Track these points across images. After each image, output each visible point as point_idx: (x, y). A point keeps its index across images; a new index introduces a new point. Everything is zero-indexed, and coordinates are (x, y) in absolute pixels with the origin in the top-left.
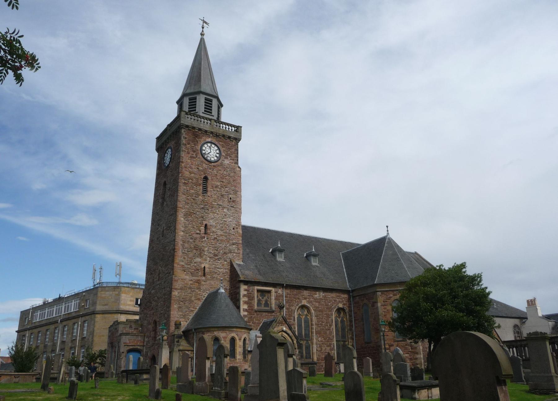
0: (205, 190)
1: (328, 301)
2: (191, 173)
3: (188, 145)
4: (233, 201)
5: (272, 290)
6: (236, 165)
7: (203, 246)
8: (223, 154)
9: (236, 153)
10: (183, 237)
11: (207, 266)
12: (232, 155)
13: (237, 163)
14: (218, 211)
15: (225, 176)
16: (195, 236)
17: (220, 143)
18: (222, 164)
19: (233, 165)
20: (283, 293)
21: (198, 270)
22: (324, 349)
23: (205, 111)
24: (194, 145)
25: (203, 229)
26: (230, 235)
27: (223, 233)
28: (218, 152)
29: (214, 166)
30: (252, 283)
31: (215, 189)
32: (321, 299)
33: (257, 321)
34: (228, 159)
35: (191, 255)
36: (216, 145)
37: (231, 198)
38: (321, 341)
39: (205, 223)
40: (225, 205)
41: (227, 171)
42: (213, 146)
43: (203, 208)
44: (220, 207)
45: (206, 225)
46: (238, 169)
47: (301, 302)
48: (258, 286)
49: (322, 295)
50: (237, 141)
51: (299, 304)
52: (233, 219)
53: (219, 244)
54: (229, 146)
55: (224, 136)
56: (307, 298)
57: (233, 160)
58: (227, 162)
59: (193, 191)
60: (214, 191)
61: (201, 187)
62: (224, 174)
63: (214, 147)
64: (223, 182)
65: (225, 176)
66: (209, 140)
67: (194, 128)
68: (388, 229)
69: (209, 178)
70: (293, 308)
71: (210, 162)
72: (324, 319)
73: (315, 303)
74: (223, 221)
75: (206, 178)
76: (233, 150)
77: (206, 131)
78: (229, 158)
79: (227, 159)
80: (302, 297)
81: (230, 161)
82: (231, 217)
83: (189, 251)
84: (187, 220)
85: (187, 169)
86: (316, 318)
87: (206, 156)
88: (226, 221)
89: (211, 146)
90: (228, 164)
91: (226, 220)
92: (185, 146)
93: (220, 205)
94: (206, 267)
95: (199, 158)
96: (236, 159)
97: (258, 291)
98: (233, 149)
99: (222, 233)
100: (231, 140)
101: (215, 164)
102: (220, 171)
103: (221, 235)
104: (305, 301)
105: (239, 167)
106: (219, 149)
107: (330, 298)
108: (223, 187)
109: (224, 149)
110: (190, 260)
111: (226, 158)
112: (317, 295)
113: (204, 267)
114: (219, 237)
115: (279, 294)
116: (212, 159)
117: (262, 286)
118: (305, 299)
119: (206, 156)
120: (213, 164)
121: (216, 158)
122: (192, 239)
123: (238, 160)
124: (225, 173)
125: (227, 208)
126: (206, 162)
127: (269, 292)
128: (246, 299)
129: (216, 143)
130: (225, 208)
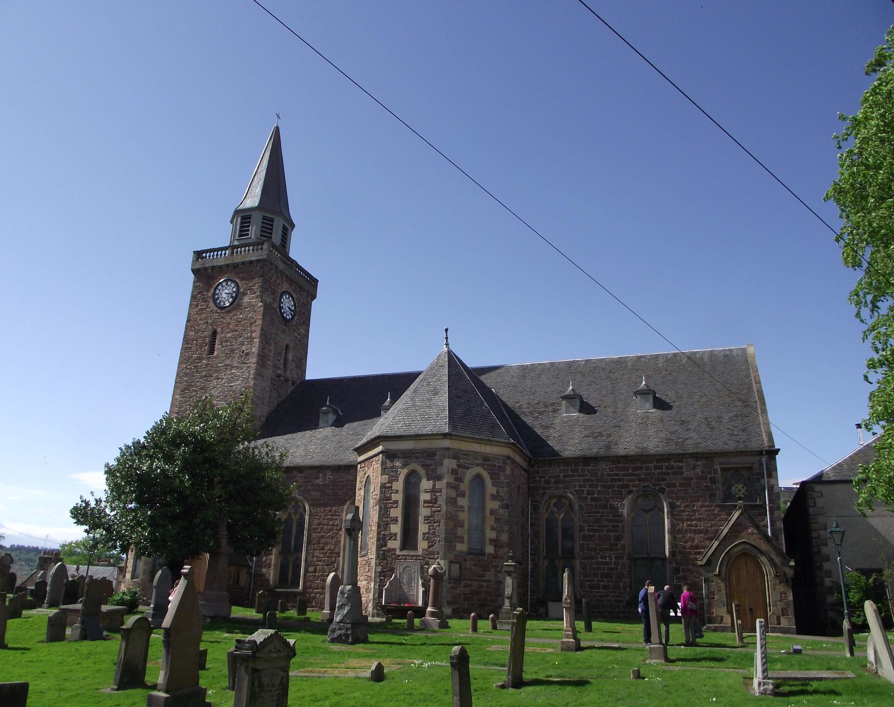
0: (212, 351)
4: (248, 354)
15: (241, 322)
17: (241, 275)
31: (224, 344)
32: (325, 485)
36: (233, 281)
40: (235, 364)
44: (227, 369)
55: (243, 263)
59: (196, 356)
60: (223, 347)
64: (236, 331)
65: (241, 322)
67: (206, 269)
68: (447, 335)
69: (219, 330)
73: (313, 493)
75: (215, 333)
85: (193, 329)
87: (218, 302)
93: (228, 366)
107: (343, 482)
109: (243, 282)
112: (319, 479)
119: (218, 302)
124: (241, 316)
125: (236, 367)
126: (219, 311)
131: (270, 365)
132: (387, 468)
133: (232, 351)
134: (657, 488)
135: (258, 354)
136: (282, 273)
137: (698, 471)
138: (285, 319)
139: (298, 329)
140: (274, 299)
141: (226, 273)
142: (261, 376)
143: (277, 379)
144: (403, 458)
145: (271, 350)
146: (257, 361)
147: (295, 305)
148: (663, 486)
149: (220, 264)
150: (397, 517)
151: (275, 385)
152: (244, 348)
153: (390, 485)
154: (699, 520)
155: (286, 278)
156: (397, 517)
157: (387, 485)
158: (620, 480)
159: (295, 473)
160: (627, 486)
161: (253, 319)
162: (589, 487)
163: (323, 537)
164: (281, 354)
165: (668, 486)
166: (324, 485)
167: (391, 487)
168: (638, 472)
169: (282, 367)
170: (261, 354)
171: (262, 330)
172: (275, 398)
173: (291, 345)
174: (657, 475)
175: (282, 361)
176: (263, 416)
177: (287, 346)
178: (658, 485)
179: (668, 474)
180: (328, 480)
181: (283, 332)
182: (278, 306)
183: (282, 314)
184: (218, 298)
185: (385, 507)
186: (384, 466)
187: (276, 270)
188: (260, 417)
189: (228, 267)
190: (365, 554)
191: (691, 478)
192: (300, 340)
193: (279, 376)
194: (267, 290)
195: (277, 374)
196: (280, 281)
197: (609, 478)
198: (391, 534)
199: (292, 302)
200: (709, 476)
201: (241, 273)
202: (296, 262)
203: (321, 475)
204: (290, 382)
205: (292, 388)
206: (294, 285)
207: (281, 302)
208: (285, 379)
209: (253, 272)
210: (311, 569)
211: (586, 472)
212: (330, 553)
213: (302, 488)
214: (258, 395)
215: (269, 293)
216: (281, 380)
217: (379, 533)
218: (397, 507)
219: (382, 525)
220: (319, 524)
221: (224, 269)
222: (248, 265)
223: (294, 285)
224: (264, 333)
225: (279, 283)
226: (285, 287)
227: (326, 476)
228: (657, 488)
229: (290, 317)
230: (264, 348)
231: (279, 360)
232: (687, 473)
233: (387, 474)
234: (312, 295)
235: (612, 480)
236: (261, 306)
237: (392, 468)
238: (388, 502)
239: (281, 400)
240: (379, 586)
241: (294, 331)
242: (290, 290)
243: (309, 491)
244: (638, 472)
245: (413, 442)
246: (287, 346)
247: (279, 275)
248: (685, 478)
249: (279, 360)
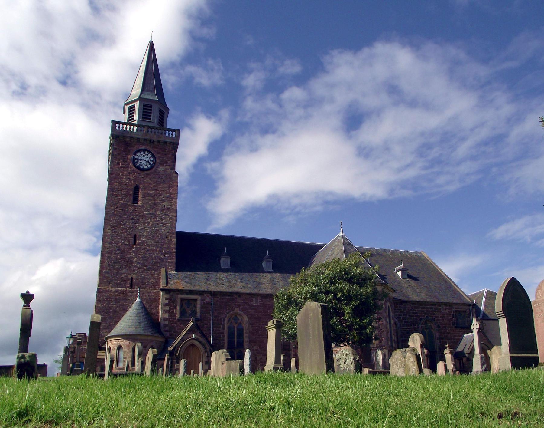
0: (136, 201)
1: (268, 308)
2: (121, 184)
3: (118, 156)
4: (168, 209)
5: (198, 298)
6: (173, 171)
7: (132, 257)
8: (158, 161)
9: (173, 158)
11: (134, 276)
12: (169, 161)
13: (174, 168)
14: (150, 220)
16: (122, 247)
17: (156, 149)
18: (156, 171)
19: (170, 171)
20: (211, 301)
21: (124, 281)
22: (258, 358)
23: (143, 118)
24: (126, 154)
25: (132, 240)
28: (152, 159)
29: (147, 174)
30: (175, 292)
33: (179, 330)
34: (163, 165)
35: (117, 266)
36: (150, 152)
37: (164, 206)
38: (256, 350)
41: (161, 178)
42: (147, 153)
43: (132, 219)
45: (135, 236)
46: (175, 175)
47: (233, 310)
48: (181, 294)
49: (260, 301)
50: (175, 145)
53: (149, 254)
54: (165, 151)
56: (241, 306)
57: (169, 166)
58: (161, 169)
61: (132, 198)
62: (159, 182)
63: (147, 155)
65: (160, 184)
66: (143, 147)
69: (141, 186)
70: (223, 316)
71: (143, 170)
72: (262, 327)
73: (250, 310)
75: (137, 189)
76: (170, 155)
77: (138, 139)
78: (164, 164)
79: (163, 166)
80: (235, 304)
81: (165, 167)
82: (165, 226)
84: (114, 232)
86: (251, 326)
88: (158, 230)
89: (145, 154)
90: (163, 171)
91: (158, 229)
92: (115, 157)
94: (133, 278)
95: (131, 167)
96: (173, 164)
97: (182, 300)
98: (169, 154)
99: (153, 242)
101: (148, 172)
102: (154, 179)
103: (152, 245)
104: (238, 308)
105: (176, 173)
106: (153, 156)
107: (270, 304)
108: (156, 195)
109: (159, 155)
110: (116, 271)
111: (161, 164)
112: (253, 301)
113: (132, 278)
114: (149, 246)
115: (206, 301)
116: (146, 167)
118: (239, 306)
119: (138, 165)
120: (146, 172)
121: (149, 166)
122: (118, 250)
123: (175, 166)
126: (139, 171)
127: (196, 300)
129: (151, 150)
134: (432, 318)
137: (447, 311)
141: (143, 145)
148: (434, 317)
149: (138, 137)
152: (165, 204)
154: (448, 333)
158: (416, 313)
159: (236, 296)
160: (419, 316)
162: (403, 316)
165: (436, 317)
168: (424, 310)
174: (432, 312)
178: (432, 316)
179: (436, 312)
184: (137, 162)
189: (144, 141)
191: (445, 314)
197: (411, 312)
200: (451, 314)
201: (156, 148)
203: (254, 299)
209: (166, 150)
211: (401, 308)
221: (141, 141)
222: (162, 144)
227: (258, 300)
228: (432, 318)
232: (444, 312)
235: (413, 313)
243: (247, 308)
244: (424, 310)
248: (442, 314)
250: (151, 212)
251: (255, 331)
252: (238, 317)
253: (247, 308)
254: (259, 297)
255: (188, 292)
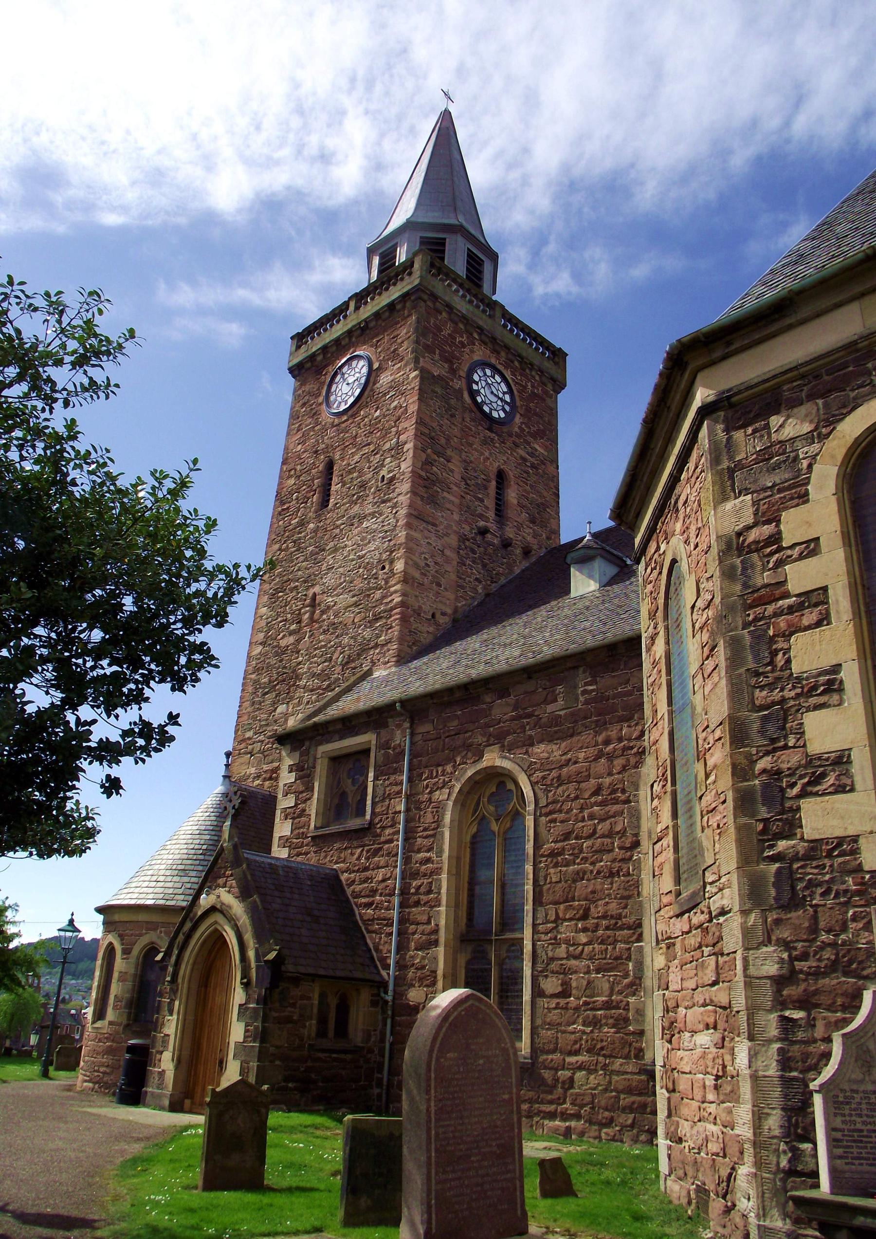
1: (621, 713)
5: (370, 741)
7: (300, 663)
10: (259, 659)
26: (369, 596)
27: (353, 596)
37: (383, 477)
39: (311, 592)
40: (369, 509)
51: (466, 770)
52: (383, 538)
74: (354, 562)
83: (267, 693)
88: (363, 556)
100: (399, 311)
115: (394, 749)
117: (341, 738)
128: (290, 801)
130: (365, 517)
131: (452, 502)
132: (739, 466)
133: (363, 486)
135: (412, 472)
136: (464, 319)
138: (488, 417)
139: (529, 443)
140: (453, 371)
142: (428, 523)
143: (479, 538)
144: (811, 397)
145: (452, 471)
146: (412, 486)
147: (510, 391)
150: (836, 668)
151: (474, 552)
153: (767, 530)
155: (479, 334)
156: (836, 668)
157: (753, 535)
161: (401, 407)
163: (579, 876)
164: (486, 488)
166: (572, 714)
167: (775, 538)
169: (491, 514)
170: (423, 474)
171: (420, 422)
172: (477, 579)
173: (512, 473)
175: (490, 502)
176: (444, 614)
177: (501, 476)
180: (581, 699)
181: (485, 442)
182: (464, 387)
183: (479, 407)
185: (758, 637)
186: (725, 464)
187: (449, 313)
188: (433, 615)
190: (694, 894)
192: (533, 466)
193: (483, 532)
194: (429, 349)
195: (479, 528)
196: (464, 339)
198: (810, 761)
199: (503, 384)
202: (502, 307)
203: (559, 688)
204: (518, 551)
205: (525, 564)
206: (503, 354)
207: (470, 381)
208: (502, 541)
210: (551, 985)
212: (607, 928)
213: (510, 738)
214: (422, 564)
215: (437, 357)
216: (490, 544)
217: (740, 772)
218: (824, 620)
219: (756, 726)
220: (567, 836)
223: (503, 354)
224: (427, 431)
225: (461, 342)
226: (479, 353)
227: (576, 687)
229: (502, 415)
230: (428, 463)
231: (482, 501)
233: (745, 491)
234: (553, 380)
236: (415, 377)
237: (764, 456)
238: (771, 609)
239: (494, 587)
240: (785, 1063)
241: (517, 446)
242: (493, 361)
245: (855, 307)
246: (501, 476)
247: (461, 326)
249: (482, 501)
250: (352, 512)
251: (564, 841)
252: (511, 786)
253: (530, 736)
254: (581, 669)
255: (339, 726)
